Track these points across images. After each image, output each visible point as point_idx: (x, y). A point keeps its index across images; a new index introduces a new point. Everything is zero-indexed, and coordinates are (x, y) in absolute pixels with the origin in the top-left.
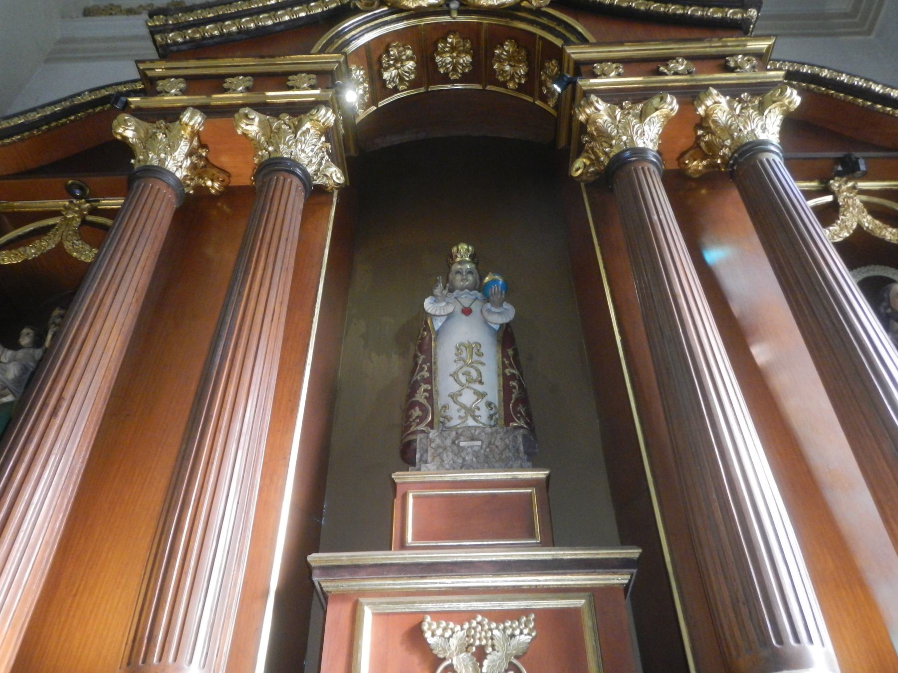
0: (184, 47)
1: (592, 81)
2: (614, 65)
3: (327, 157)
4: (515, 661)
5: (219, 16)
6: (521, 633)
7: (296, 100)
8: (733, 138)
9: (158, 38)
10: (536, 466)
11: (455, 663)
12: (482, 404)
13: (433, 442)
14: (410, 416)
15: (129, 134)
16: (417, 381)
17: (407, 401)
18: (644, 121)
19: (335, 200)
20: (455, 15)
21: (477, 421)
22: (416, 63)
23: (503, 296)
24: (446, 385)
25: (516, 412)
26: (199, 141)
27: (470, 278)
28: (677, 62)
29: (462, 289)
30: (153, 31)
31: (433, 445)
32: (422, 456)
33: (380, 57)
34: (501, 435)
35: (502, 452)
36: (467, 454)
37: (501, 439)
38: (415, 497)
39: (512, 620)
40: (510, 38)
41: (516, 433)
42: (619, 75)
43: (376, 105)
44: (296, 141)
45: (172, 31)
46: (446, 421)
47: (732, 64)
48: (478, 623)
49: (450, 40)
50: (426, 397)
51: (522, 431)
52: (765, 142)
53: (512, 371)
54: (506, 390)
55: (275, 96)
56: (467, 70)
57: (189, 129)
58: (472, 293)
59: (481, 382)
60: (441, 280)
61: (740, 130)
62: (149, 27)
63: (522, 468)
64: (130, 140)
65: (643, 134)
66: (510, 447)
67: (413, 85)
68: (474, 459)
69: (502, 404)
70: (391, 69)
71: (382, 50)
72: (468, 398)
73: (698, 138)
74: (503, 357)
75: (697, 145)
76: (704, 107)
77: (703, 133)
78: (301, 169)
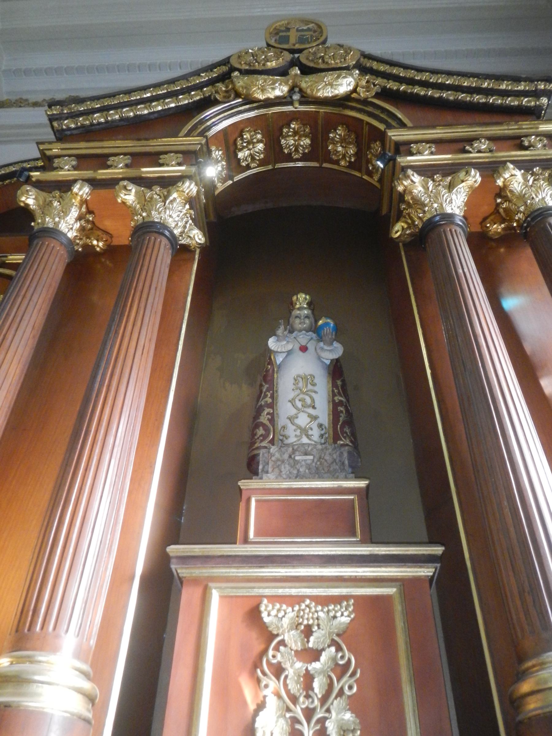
0: (75, 132)
1: (409, 158)
2: (428, 145)
3: (190, 221)
4: (336, 639)
5: (104, 106)
6: (342, 615)
7: (166, 175)
9: (55, 124)
10: (358, 477)
11: (286, 638)
12: (314, 425)
13: (274, 456)
14: (255, 435)
15: (31, 201)
16: (261, 406)
17: (254, 421)
18: (452, 191)
19: (197, 256)
20: (297, 105)
21: (310, 439)
22: (265, 145)
23: (334, 337)
25: (343, 432)
26: (87, 208)
27: (307, 321)
28: (481, 142)
29: (300, 331)
30: (52, 119)
31: (273, 458)
32: (264, 467)
33: (235, 140)
34: (330, 451)
35: (330, 465)
36: (301, 466)
37: (330, 454)
38: (257, 501)
40: (343, 124)
41: (342, 449)
42: (432, 153)
43: (232, 180)
44: (165, 208)
45: (66, 119)
46: (284, 439)
47: (526, 143)
48: (307, 606)
49: (293, 126)
50: (268, 419)
51: (347, 448)
53: (340, 398)
54: (335, 415)
55: (149, 171)
56: (306, 151)
57: (79, 198)
58: (308, 334)
59: (314, 407)
60: (282, 323)
61: (533, 198)
62: (48, 115)
63: (346, 478)
64: (31, 207)
65: (451, 202)
66: (337, 461)
67: (262, 163)
68: (307, 471)
69: (332, 425)
70: (245, 150)
71: (237, 134)
72: (303, 420)
73: (498, 205)
74: (333, 386)
75: (496, 211)
76: (502, 179)
77: (501, 202)
78: (169, 231)
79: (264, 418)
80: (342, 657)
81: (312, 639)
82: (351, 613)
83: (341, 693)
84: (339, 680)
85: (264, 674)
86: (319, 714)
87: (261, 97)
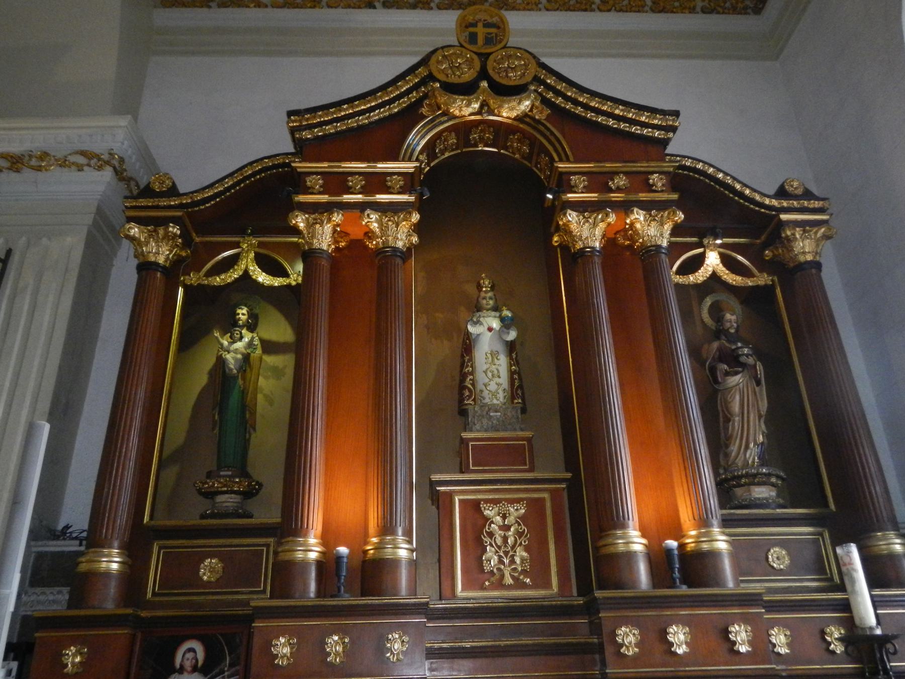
6: (521, 508)
8: (643, 240)
12: (500, 391)
16: (465, 373)
21: (498, 400)
24: (481, 378)
29: (488, 310)
30: (293, 131)
32: (472, 419)
39: (517, 503)
45: (305, 130)
50: (471, 384)
52: (660, 247)
54: (512, 381)
59: (499, 377)
62: (291, 127)
79: (468, 383)
80: (521, 529)
81: (506, 520)
82: (525, 507)
83: (521, 544)
85: (485, 537)
86: (511, 553)
87: (457, 113)
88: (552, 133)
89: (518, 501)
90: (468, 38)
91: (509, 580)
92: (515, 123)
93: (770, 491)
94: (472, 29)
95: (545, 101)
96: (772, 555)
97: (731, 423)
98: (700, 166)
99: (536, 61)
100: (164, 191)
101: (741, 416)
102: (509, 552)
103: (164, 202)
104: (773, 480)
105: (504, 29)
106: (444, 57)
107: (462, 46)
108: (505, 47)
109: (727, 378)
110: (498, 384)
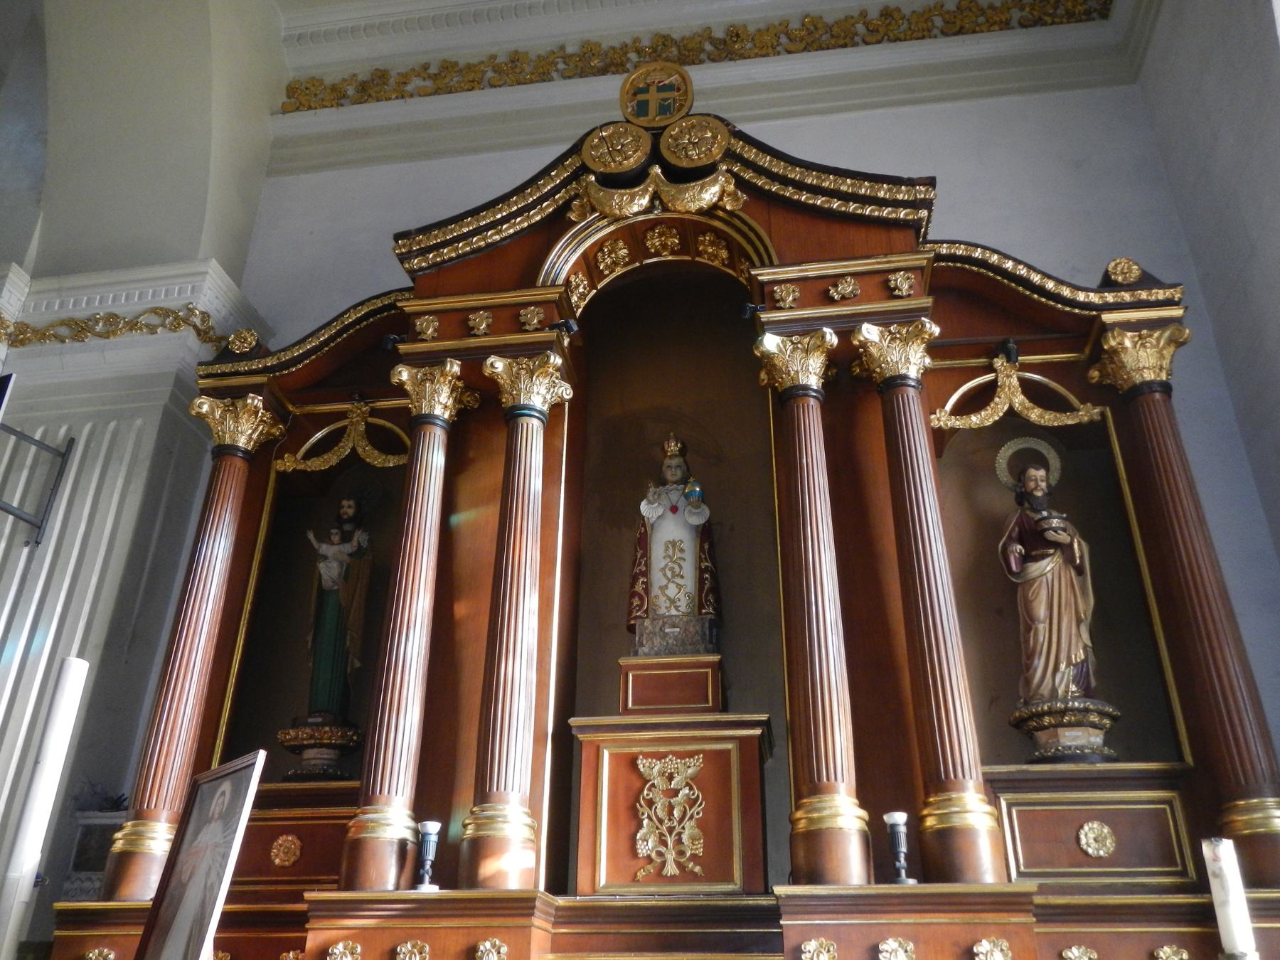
4: (690, 782)
11: (656, 782)
12: (681, 595)
21: (678, 610)
24: (657, 578)
32: (640, 638)
33: (596, 255)
43: (596, 288)
45: (417, 257)
51: (709, 616)
52: (905, 377)
54: (701, 581)
59: (682, 577)
62: (398, 255)
72: (672, 591)
79: (639, 588)
80: (693, 794)
81: (673, 782)
84: (690, 809)
86: (678, 830)
88: (752, 229)
89: (691, 755)
90: (635, 108)
91: (671, 869)
92: (702, 219)
93: (1090, 735)
94: (641, 97)
95: (741, 183)
96: (1086, 835)
97: (1032, 634)
98: (978, 254)
99: (729, 131)
100: (246, 352)
101: (1048, 621)
102: (674, 827)
103: (243, 367)
104: (1094, 718)
105: (686, 92)
106: (603, 138)
107: (628, 121)
108: (687, 115)
109: (1030, 564)
110: (679, 587)
